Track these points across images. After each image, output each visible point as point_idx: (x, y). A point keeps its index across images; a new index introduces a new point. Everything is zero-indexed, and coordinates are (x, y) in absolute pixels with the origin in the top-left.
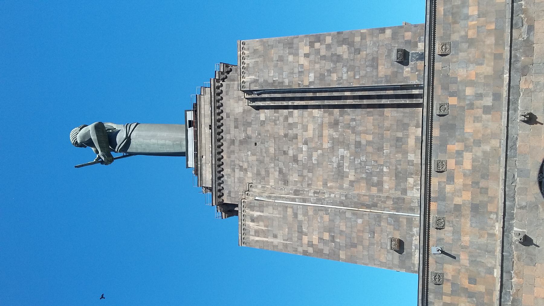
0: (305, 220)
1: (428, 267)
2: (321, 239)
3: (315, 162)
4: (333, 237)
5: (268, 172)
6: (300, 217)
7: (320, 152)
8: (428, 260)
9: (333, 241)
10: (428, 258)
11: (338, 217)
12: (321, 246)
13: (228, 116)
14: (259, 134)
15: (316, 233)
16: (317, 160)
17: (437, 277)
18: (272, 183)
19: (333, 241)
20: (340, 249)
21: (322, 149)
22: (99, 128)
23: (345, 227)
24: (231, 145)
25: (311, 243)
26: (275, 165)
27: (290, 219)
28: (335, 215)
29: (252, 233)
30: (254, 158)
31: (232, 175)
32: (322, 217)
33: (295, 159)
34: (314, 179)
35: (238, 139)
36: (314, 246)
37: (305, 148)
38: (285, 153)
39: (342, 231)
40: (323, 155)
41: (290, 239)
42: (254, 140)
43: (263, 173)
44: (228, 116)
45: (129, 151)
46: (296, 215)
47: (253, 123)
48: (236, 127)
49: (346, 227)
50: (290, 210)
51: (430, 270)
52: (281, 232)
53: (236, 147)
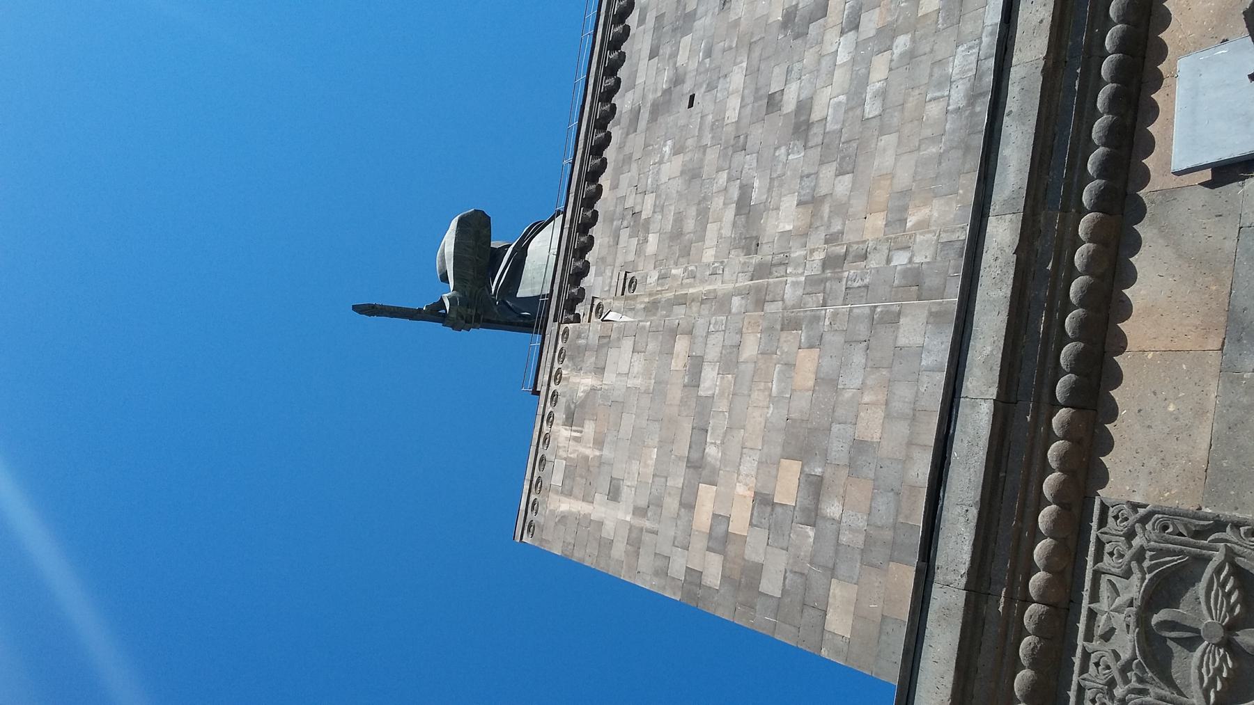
0: (722, 393)
1: (1091, 442)
2: (763, 500)
3: (871, 109)
4: (815, 487)
5: (703, 216)
6: (710, 379)
7: (902, 43)
8: (1108, 305)
9: (812, 515)
10: (1114, 271)
11: (858, 358)
12: (756, 549)
13: (642, 21)
14: (709, 53)
15: (749, 466)
16: (883, 94)
17: (1203, 606)
18: (709, 255)
19: (812, 515)
20: (832, 572)
21: (913, 25)
22: (475, 229)
23: (880, 413)
24: (628, 134)
25: (720, 530)
26: (729, 180)
27: (675, 393)
28: (848, 342)
29: (557, 479)
30: (679, 161)
31: (609, 260)
32: (790, 366)
33: (802, 126)
34: (858, 205)
35: (650, 97)
36: (732, 549)
37: (843, 48)
38: (773, 102)
39: (859, 447)
40: (911, 56)
41: (657, 503)
42: (687, 88)
43: (690, 225)
44: (642, 21)
45: (522, 292)
46: (696, 366)
48: (653, 54)
49: (888, 416)
50: (681, 345)
51: (1129, 478)
52: (635, 466)
53: (637, 140)
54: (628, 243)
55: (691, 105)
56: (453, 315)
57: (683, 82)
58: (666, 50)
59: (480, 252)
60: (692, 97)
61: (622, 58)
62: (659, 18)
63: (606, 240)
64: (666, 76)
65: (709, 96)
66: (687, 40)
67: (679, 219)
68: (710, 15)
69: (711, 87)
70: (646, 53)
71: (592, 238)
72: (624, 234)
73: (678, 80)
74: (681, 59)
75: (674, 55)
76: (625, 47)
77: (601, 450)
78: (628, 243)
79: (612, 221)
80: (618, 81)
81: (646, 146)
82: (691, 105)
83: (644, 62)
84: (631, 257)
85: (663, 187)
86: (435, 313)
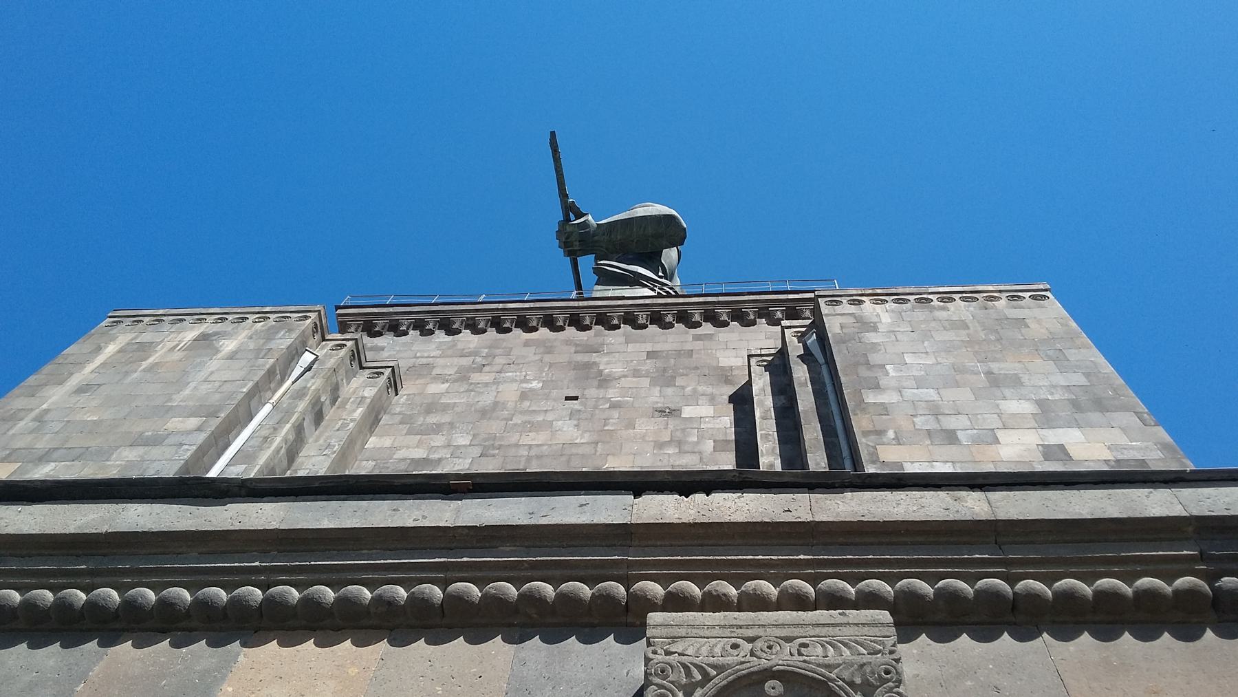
22: (667, 232)
31: (449, 352)
47: (670, 391)
54: (449, 366)
55: (567, 399)
56: (568, 229)
57: (599, 386)
58: (649, 365)
59: (645, 242)
60: (576, 398)
61: (667, 326)
62: (690, 353)
63: (472, 346)
64: (618, 369)
65: (566, 413)
66: (645, 382)
67: (446, 408)
68: (656, 399)
69: (572, 414)
70: (658, 347)
71: (484, 331)
72: (465, 362)
73: (605, 382)
74: (628, 382)
75: (636, 373)
76: (680, 327)
77: (144, 370)
78: (449, 366)
79: (490, 347)
80: (644, 327)
81: (551, 365)
82: (567, 399)
83: (649, 347)
84: (436, 371)
85: (494, 387)
86: (570, 210)
